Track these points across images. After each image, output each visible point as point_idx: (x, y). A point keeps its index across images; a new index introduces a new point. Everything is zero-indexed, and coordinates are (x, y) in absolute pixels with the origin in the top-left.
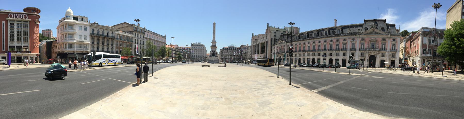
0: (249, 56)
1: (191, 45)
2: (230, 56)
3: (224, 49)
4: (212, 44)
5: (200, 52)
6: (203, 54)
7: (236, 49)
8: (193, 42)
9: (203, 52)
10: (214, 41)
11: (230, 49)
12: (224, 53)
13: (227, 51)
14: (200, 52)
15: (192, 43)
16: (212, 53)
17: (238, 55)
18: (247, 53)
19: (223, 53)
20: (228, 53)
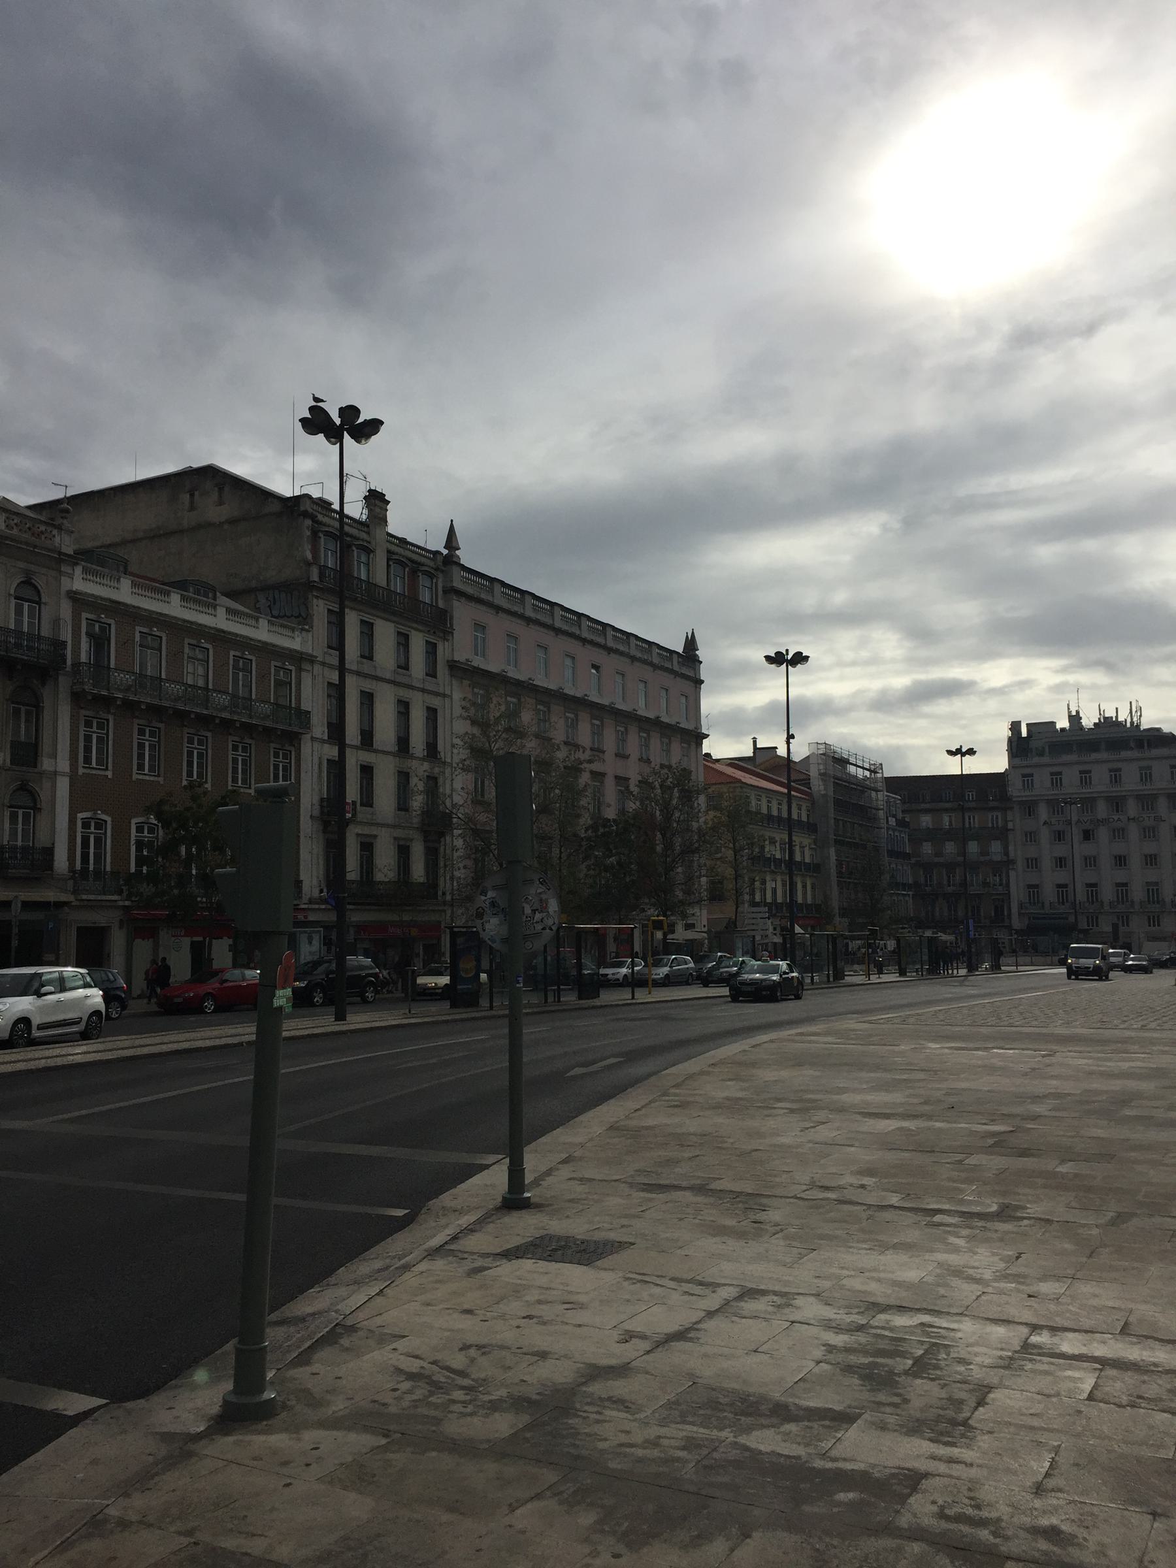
5: (1134, 832)
8: (1028, 716)
14: (1134, 832)
15: (1015, 726)
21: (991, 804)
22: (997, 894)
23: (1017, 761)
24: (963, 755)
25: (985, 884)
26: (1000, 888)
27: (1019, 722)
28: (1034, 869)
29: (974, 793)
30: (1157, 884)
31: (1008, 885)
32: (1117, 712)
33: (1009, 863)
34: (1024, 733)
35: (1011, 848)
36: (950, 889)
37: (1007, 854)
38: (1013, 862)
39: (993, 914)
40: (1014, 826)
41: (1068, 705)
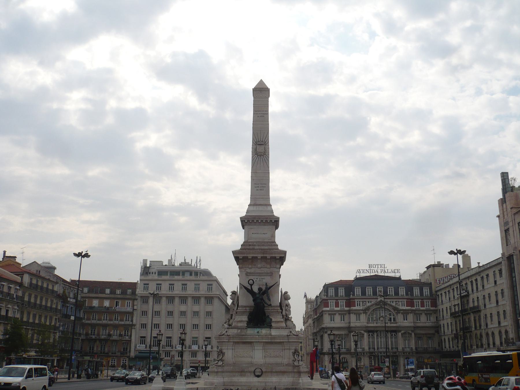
0: (493, 325)
1: (139, 271)
2: (366, 335)
3: (332, 292)
4: (246, 235)
6: (209, 327)
7: (402, 291)
9: (209, 314)
10: (260, 212)
11: (364, 293)
12: (332, 320)
13: (350, 303)
16: (247, 301)
17: (416, 328)
18: (476, 310)
19: (326, 318)
20: (353, 317)
21: (128, 297)
22: (125, 340)
23: (143, 278)
24: (83, 256)
25: (121, 335)
26: (127, 337)
27: (147, 260)
28: (144, 329)
29: (120, 291)
30: (197, 338)
31: (131, 336)
32: (192, 261)
33: (133, 326)
34: (148, 265)
35: (134, 318)
36: (103, 337)
37: (132, 321)
38: (135, 325)
39: (122, 350)
40: (137, 308)
41: (171, 256)
